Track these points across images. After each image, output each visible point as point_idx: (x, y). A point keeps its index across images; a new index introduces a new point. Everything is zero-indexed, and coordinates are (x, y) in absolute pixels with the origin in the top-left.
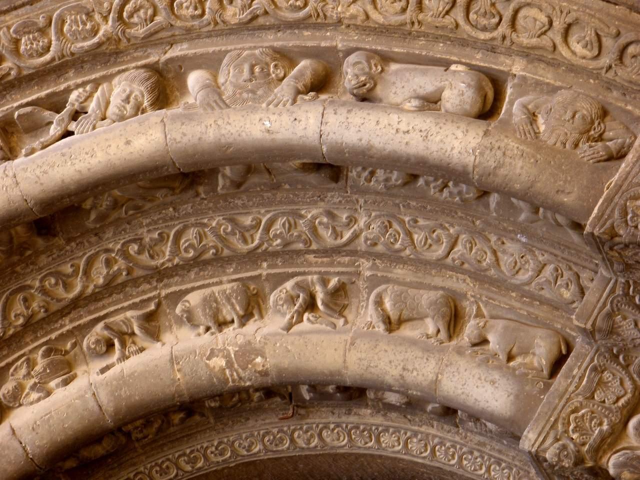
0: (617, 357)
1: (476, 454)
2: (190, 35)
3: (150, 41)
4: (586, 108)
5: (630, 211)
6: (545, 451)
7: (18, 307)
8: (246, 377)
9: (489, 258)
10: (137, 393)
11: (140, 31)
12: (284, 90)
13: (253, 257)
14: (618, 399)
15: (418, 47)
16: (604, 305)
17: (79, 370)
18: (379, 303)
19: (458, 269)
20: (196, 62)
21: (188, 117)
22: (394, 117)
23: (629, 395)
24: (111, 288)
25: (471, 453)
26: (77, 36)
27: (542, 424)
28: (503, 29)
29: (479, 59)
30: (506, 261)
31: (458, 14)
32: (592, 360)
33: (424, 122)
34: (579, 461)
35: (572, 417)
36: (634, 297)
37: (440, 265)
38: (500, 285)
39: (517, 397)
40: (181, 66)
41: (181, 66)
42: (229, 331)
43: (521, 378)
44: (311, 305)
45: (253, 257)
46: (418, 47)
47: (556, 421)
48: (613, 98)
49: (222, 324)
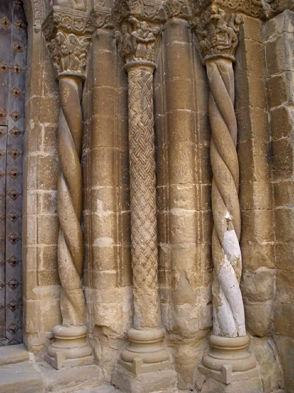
0: (88, 24)
1: (40, 5)
5: (136, 2)
6: (55, 13)
14: (77, 28)
16: (102, 12)
23: (79, 31)
25: (39, 4)
27: (62, 10)
32: (84, 17)
34: (56, 23)
35: (68, 17)
36: (107, 20)
39: (65, 3)
47: (65, 13)
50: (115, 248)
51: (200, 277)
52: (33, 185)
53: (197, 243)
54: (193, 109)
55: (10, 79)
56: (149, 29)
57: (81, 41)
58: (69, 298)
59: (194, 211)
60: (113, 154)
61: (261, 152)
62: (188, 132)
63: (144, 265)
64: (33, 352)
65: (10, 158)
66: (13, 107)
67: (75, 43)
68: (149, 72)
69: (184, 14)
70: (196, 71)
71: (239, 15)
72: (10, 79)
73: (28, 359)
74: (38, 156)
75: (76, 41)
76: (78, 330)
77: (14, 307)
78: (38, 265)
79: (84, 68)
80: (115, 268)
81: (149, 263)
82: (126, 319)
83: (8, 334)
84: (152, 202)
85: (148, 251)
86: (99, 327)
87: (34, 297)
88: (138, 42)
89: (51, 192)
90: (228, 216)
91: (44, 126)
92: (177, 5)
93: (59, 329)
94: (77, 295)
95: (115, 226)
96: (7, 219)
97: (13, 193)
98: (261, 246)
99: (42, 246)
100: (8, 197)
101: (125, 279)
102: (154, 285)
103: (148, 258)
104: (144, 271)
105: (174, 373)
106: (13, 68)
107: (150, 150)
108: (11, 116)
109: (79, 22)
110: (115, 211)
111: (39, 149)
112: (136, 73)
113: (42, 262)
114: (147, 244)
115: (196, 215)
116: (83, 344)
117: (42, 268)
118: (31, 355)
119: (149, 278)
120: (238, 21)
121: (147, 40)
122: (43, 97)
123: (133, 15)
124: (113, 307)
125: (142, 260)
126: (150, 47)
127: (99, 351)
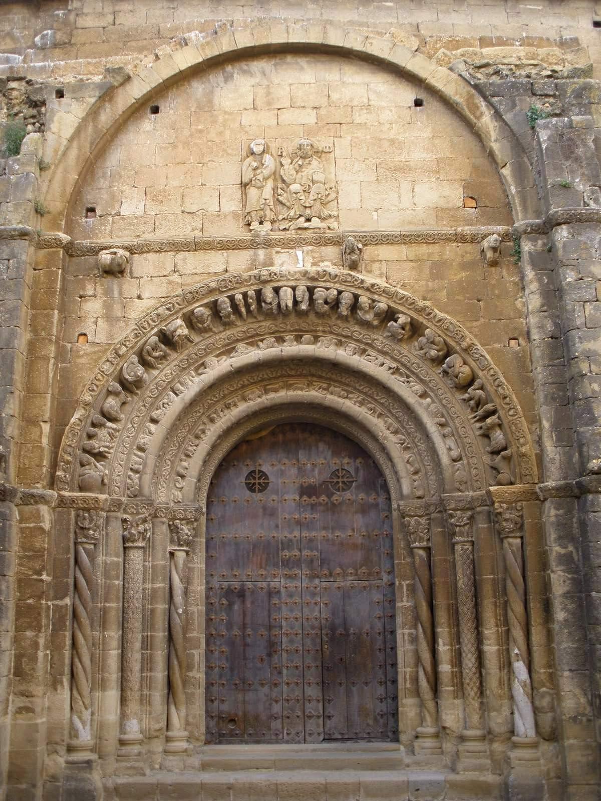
2: (436, 395)
3: (430, 388)
4: (465, 479)
7: (367, 389)
8: (381, 441)
9: (430, 474)
10: (365, 422)
11: (430, 385)
12: (437, 420)
13: (404, 428)
15: (459, 441)
17: (363, 407)
18: (410, 457)
19: (426, 469)
20: (431, 398)
21: (420, 404)
22: (442, 444)
24: (382, 404)
26: (422, 374)
28: (470, 456)
29: (463, 454)
30: (432, 477)
31: (468, 446)
33: (445, 451)
34: (404, 513)
37: (424, 465)
38: (427, 479)
40: (429, 396)
41: (429, 396)
42: (388, 432)
43: (412, 492)
44: (402, 444)
45: (404, 428)
46: (459, 441)
48: (469, 483)
49: (388, 429)
50: (452, 672)
51: (504, 694)
52: (400, 627)
53: (500, 670)
54: (494, 575)
55: (382, 543)
56: (464, 515)
57: (423, 521)
58: (425, 707)
59: (497, 647)
60: (449, 605)
61: (538, 605)
62: (490, 592)
63: (468, 684)
64: (403, 745)
65: (387, 604)
66: (386, 565)
67: (419, 523)
68: (468, 547)
69: (485, 503)
70: (497, 544)
71: (519, 504)
72: (382, 543)
73: (399, 750)
74: (402, 606)
75: (419, 522)
76: (431, 730)
77: (393, 714)
78: (405, 683)
79: (428, 540)
80: (453, 686)
81: (472, 684)
82: (461, 723)
83: (390, 734)
84: (473, 641)
85: (471, 674)
86: (444, 728)
87: (403, 706)
88: (457, 526)
89: (413, 631)
90: (516, 651)
91: (405, 583)
92: (478, 499)
93: (419, 729)
94: (430, 704)
95: (452, 657)
96: (387, 650)
97: (390, 630)
98: (541, 673)
99: (408, 670)
100: (386, 633)
101: (460, 694)
102: (476, 698)
103: (471, 679)
104: (469, 688)
105: (489, 762)
106: (383, 533)
107: (470, 604)
108: (385, 572)
109: (419, 509)
110: (451, 646)
111: (402, 601)
112: (458, 547)
113: (408, 682)
114: (470, 669)
115: (499, 650)
116: (434, 740)
117: (408, 685)
118: (402, 748)
119: (472, 693)
120: (519, 508)
121: (462, 524)
122: (403, 561)
123: (450, 510)
124: (451, 714)
125: (467, 681)
126: (466, 527)
127: (444, 745)
